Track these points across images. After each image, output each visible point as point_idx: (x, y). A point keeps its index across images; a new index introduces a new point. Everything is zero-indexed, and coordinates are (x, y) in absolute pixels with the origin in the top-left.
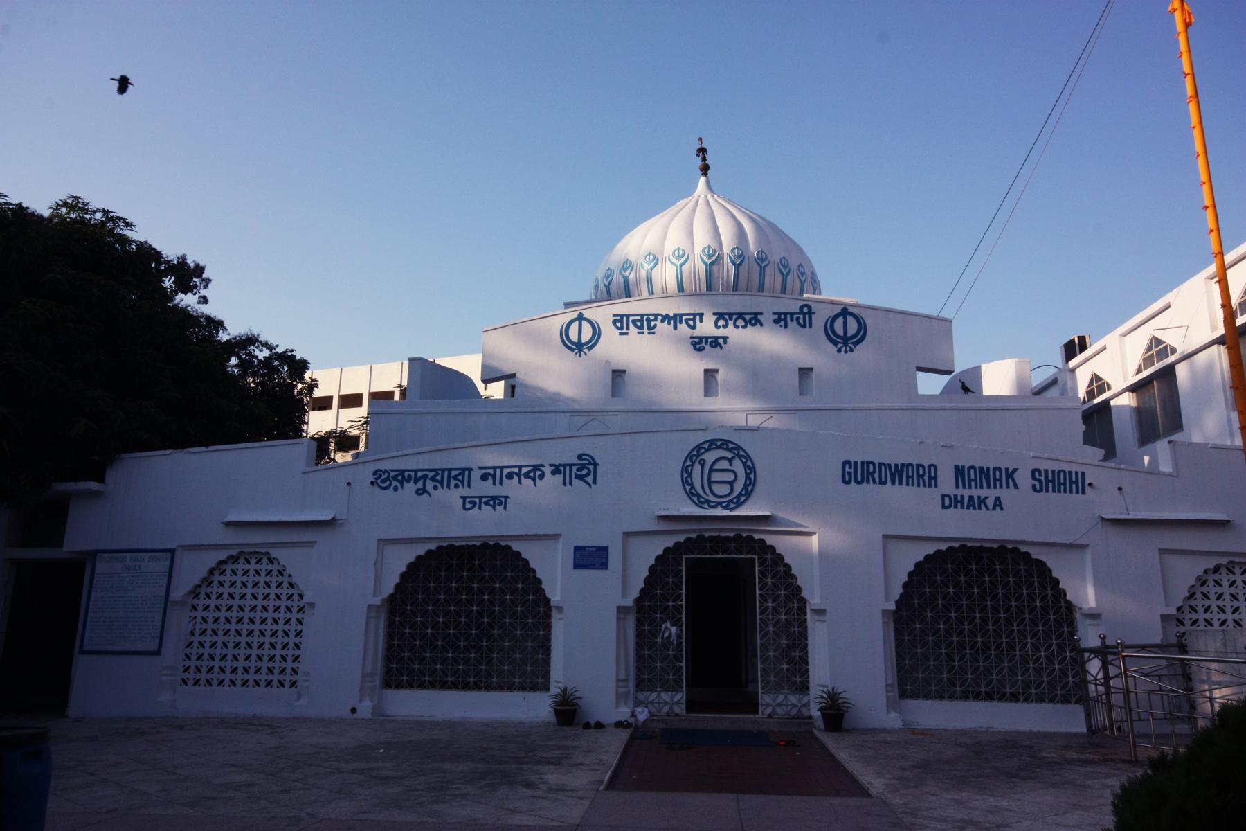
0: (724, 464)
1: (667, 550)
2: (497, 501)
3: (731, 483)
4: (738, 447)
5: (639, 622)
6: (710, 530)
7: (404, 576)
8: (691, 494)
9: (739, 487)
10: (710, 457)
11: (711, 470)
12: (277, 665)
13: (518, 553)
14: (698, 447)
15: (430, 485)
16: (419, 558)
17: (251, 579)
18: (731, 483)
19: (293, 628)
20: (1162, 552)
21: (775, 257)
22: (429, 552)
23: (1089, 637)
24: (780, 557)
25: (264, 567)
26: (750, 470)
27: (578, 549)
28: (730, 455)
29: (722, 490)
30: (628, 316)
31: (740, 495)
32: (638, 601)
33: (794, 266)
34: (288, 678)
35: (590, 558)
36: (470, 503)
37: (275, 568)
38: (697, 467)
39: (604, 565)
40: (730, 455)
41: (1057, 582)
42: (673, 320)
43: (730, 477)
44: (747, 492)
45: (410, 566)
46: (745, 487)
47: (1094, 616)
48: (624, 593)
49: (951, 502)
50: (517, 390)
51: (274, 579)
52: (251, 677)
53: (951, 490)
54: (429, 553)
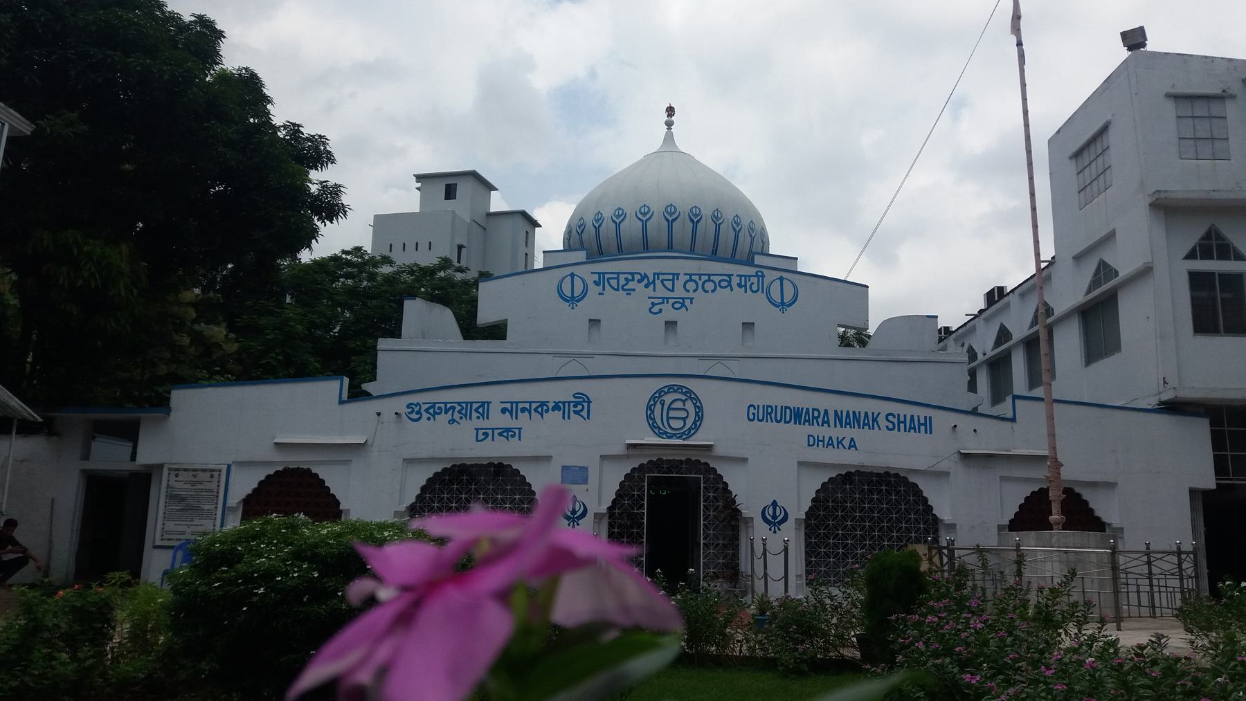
0: (679, 405)
1: (633, 470)
3: (684, 419)
4: (690, 391)
5: (611, 526)
6: (668, 456)
7: (423, 489)
8: (653, 427)
9: (689, 422)
10: (668, 399)
11: (669, 408)
13: (518, 471)
14: (660, 391)
16: (436, 474)
18: (684, 419)
20: (1003, 479)
21: (729, 215)
22: (445, 470)
23: (944, 539)
24: (721, 477)
26: (699, 409)
27: (565, 468)
28: (684, 398)
29: (677, 424)
30: (604, 274)
31: (690, 428)
32: (609, 508)
33: (745, 223)
38: (659, 406)
40: (684, 398)
41: (926, 500)
43: (683, 414)
44: (696, 427)
45: (429, 480)
46: (695, 422)
47: (952, 527)
48: (600, 505)
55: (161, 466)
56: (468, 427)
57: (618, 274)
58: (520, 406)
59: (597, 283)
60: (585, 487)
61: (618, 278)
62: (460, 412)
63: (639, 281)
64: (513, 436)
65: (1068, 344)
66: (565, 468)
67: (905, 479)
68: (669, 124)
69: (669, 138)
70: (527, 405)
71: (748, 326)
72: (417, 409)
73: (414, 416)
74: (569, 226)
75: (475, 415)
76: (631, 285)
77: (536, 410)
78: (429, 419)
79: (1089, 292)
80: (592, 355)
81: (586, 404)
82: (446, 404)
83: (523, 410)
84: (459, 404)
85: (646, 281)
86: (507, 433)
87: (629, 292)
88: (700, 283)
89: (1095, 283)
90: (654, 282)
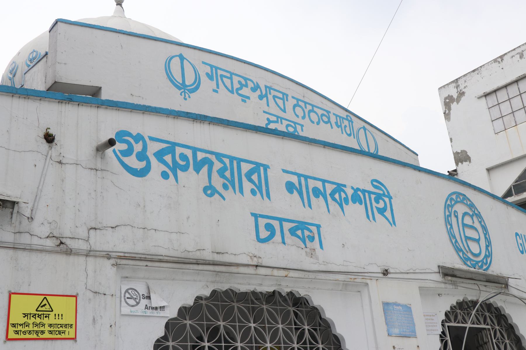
30: (217, 68)
57: (232, 74)
58: (312, 184)
59: (210, 77)
60: (412, 341)
61: (231, 78)
62: (221, 173)
63: (254, 90)
64: (312, 239)
66: (386, 305)
70: (319, 185)
72: (138, 147)
73: (132, 161)
74: (13, 62)
75: (247, 186)
76: (245, 91)
77: (332, 195)
78: (165, 176)
81: (387, 200)
82: (195, 150)
83: (317, 192)
84: (219, 156)
85: (258, 92)
86: (304, 232)
87: (245, 98)
88: (306, 111)
90: (266, 96)
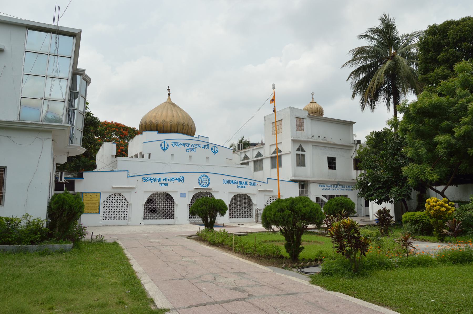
2: (166, 184)
8: (200, 184)
10: (203, 178)
12: (123, 216)
15: (153, 181)
17: (116, 199)
19: (126, 208)
25: (119, 196)
26: (209, 180)
27: (181, 194)
34: (125, 218)
35: (183, 195)
36: (161, 185)
37: (121, 196)
39: (185, 197)
41: (251, 200)
42: (184, 145)
44: (209, 184)
47: (256, 205)
49: (238, 187)
50: (151, 156)
51: (121, 199)
52: (118, 218)
53: (238, 185)
54: (153, 194)
55: (82, 193)
56: (157, 183)
65: (267, 164)
66: (181, 194)
67: (247, 196)
68: (169, 94)
69: (169, 98)
71: (207, 158)
79: (273, 154)
80: (171, 164)
89: (275, 152)
